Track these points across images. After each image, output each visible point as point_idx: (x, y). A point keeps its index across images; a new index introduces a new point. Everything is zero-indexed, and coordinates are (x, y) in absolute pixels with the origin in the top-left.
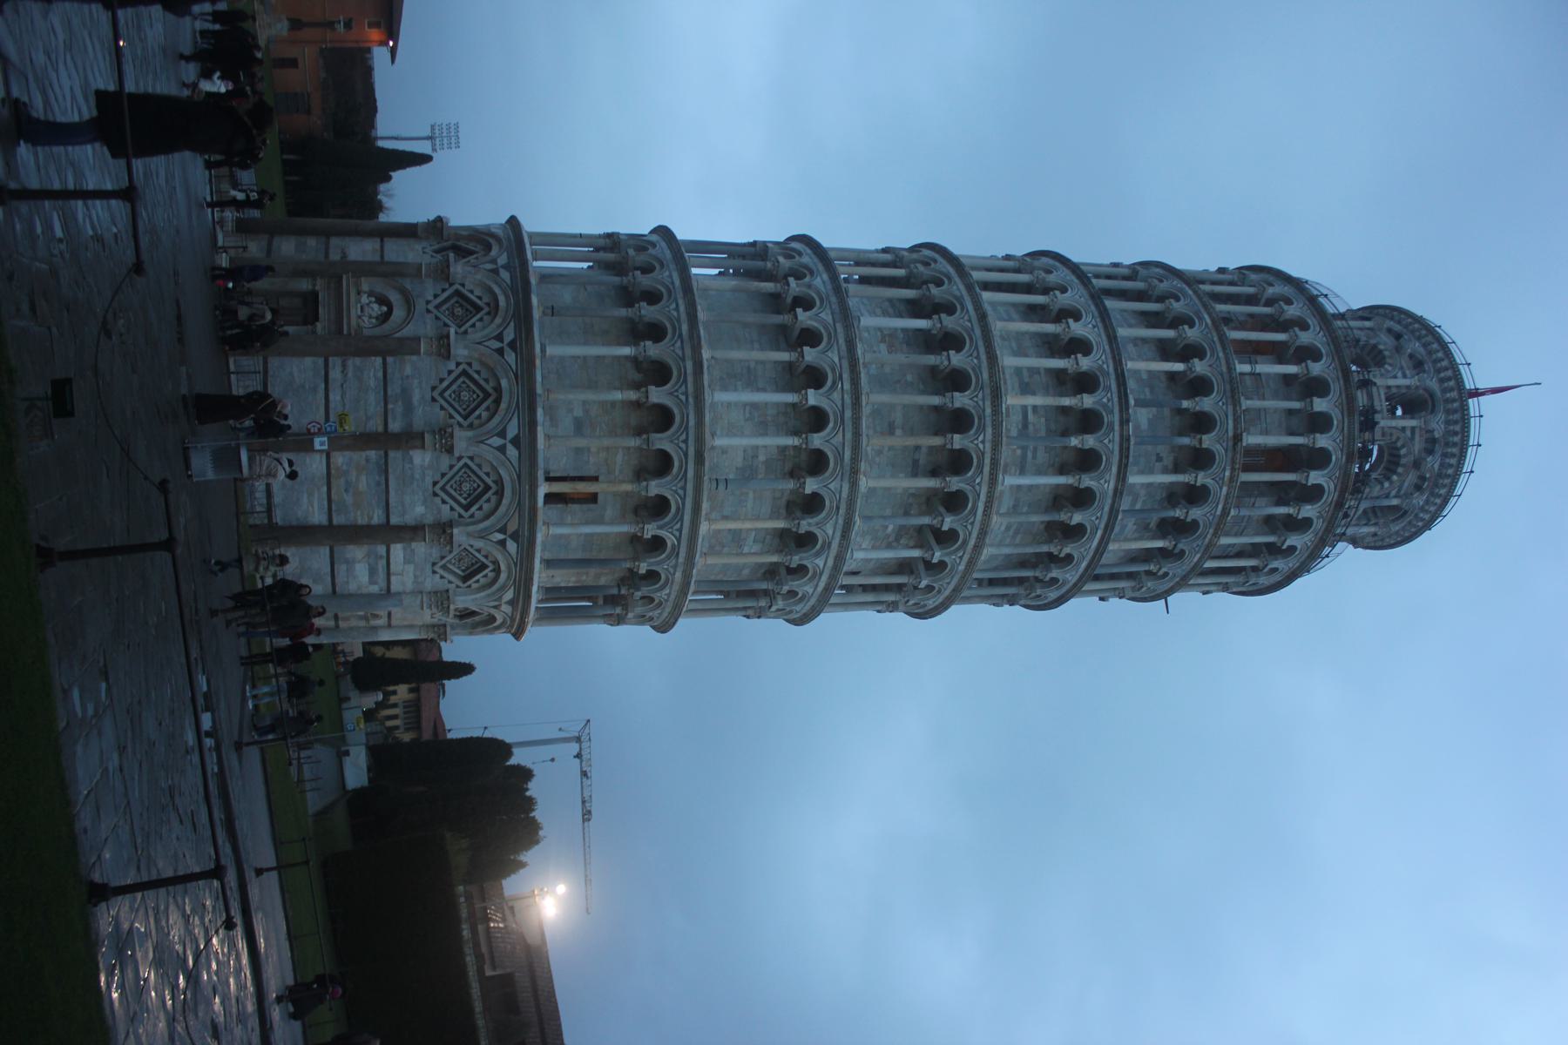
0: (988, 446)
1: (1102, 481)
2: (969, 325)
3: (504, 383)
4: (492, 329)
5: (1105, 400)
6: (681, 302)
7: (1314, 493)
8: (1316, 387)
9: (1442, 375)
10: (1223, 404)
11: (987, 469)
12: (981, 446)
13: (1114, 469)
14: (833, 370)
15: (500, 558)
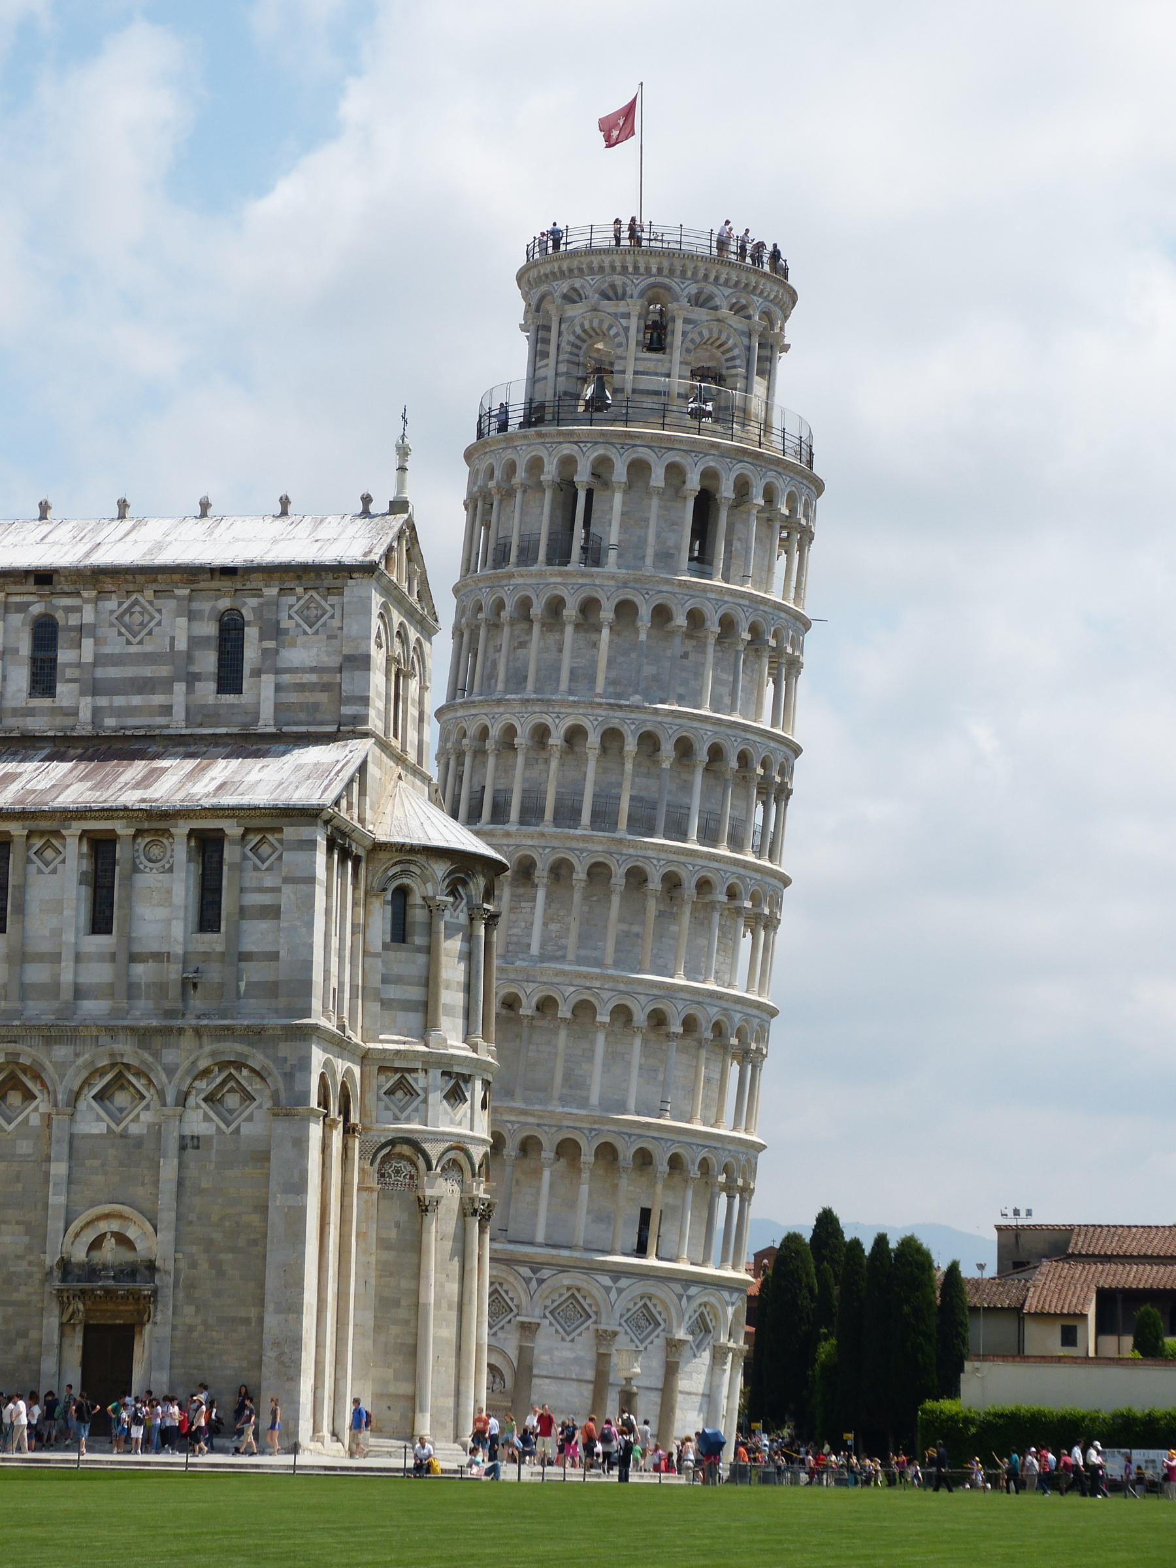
0: (663, 856)
1: (705, 737)
2: (548, 850)
3: (566, 1282)
4: (520, 1286)
5: (633, 727)
6: (506, 1118)
7: (743, 488)
8: (639, 469)
9: (630, 269)
10: (647, 593)
11: (683, 859)
12: (662, 862)
13: (696, 724)
14: (581, 993)
15: (699, 1301)
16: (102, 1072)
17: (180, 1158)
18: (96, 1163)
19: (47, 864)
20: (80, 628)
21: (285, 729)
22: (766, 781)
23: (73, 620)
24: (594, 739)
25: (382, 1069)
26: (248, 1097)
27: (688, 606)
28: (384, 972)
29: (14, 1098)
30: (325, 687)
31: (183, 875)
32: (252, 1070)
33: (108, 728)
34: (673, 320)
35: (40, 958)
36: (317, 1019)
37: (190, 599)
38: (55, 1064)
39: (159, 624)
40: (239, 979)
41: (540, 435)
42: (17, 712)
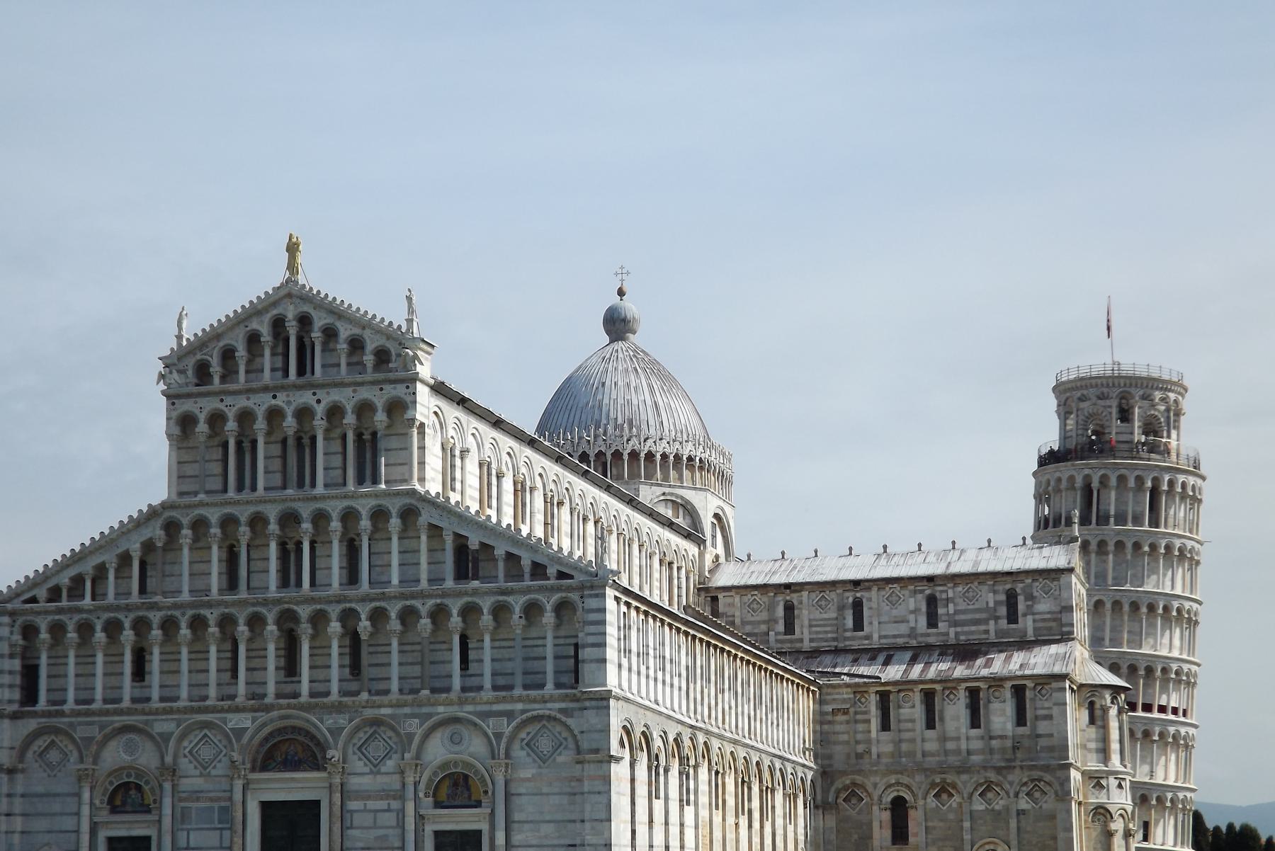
7: (1171, 483)
8: (1122, 479)
9: (1111, 385)
16: (981, 785)
17: (1018, 818)
18: (982, 822)
19: (951, 701)
20: (947, 599)
21: (1039, 638)
22: (1189, 619)
23: (944, 596)
24: (1108, 606)
25: (1090, 778)
26: (1045, 793)
27: (1149, 542)
28: (1087, 736)
29: (944, 796)
30: (1054, 620)
31: (1010, 703)
32: (1045, 782)
33: (963, 640)
34: (1133, 407)
35: (952, 739)
36: (1071, 761)
37: (994, 585)
38: (962, 782)
39: (981, 596)
40: (1037, 745)
41: (1073, 465)
42: (922, 635)
